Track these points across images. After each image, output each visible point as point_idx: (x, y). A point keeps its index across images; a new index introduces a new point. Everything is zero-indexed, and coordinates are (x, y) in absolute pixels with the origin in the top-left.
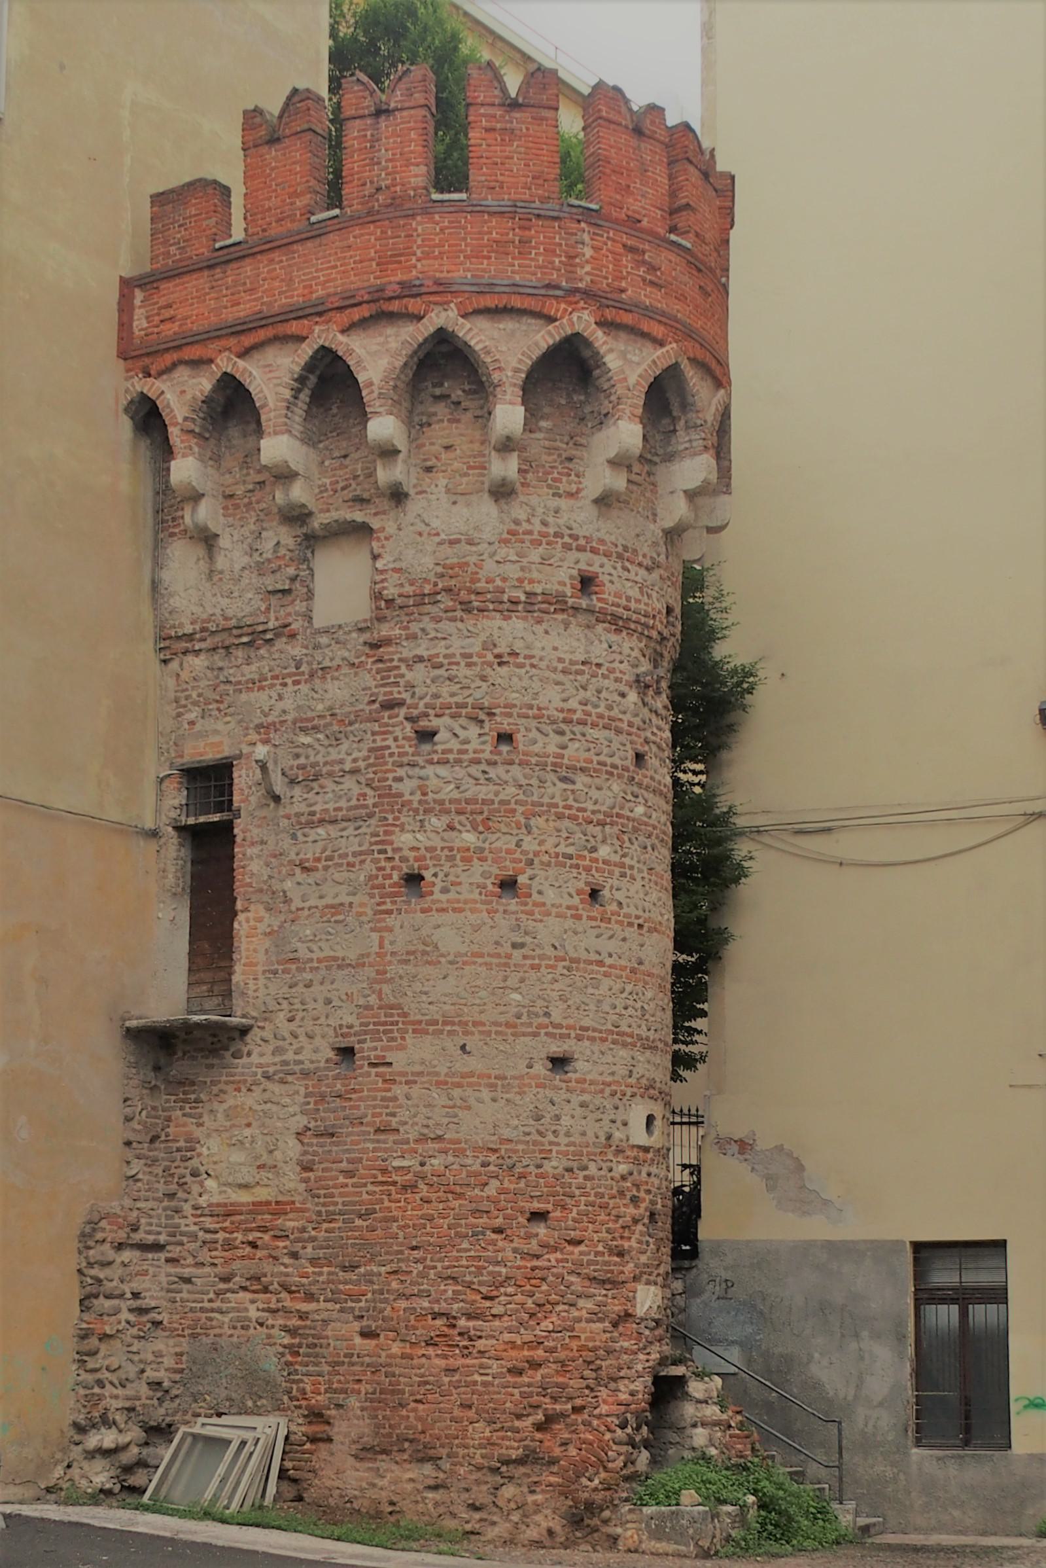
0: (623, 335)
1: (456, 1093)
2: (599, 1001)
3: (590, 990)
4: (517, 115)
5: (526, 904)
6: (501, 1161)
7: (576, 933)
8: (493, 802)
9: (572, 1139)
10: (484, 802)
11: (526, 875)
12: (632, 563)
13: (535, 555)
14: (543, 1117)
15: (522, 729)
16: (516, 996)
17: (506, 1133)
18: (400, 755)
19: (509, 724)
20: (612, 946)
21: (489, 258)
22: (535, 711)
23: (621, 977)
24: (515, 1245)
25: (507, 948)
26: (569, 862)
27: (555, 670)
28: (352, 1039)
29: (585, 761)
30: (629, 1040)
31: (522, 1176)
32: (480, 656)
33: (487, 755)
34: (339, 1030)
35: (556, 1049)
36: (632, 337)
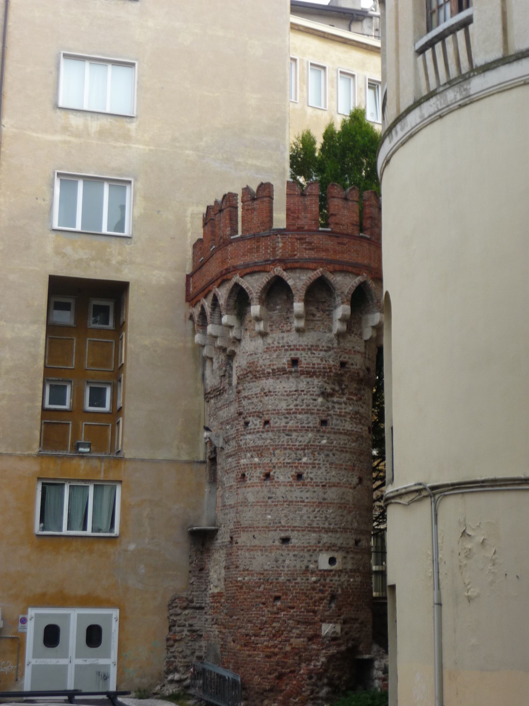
0: (298, 271)
1: (252, 553)
4: (256, 202)
5: (272, 482)
7: (291, 491)
8: (262, 446)
9: (290, 569)
10: (260, 446)
12: (316, 350)
13: (275, 356)
15: (273, 418)
16: (269, 517)
17: (266, 567)
21: (247, 255)
22: (277, 411)
24: (269, 609)
25: (267, 499)
26: (288, 466)
27: (284, 395)
29: (296, 427)
30: (317, 529)
31: (271, 583)
32: (260, 394)
33: (261, 430)
35: (283, 535)
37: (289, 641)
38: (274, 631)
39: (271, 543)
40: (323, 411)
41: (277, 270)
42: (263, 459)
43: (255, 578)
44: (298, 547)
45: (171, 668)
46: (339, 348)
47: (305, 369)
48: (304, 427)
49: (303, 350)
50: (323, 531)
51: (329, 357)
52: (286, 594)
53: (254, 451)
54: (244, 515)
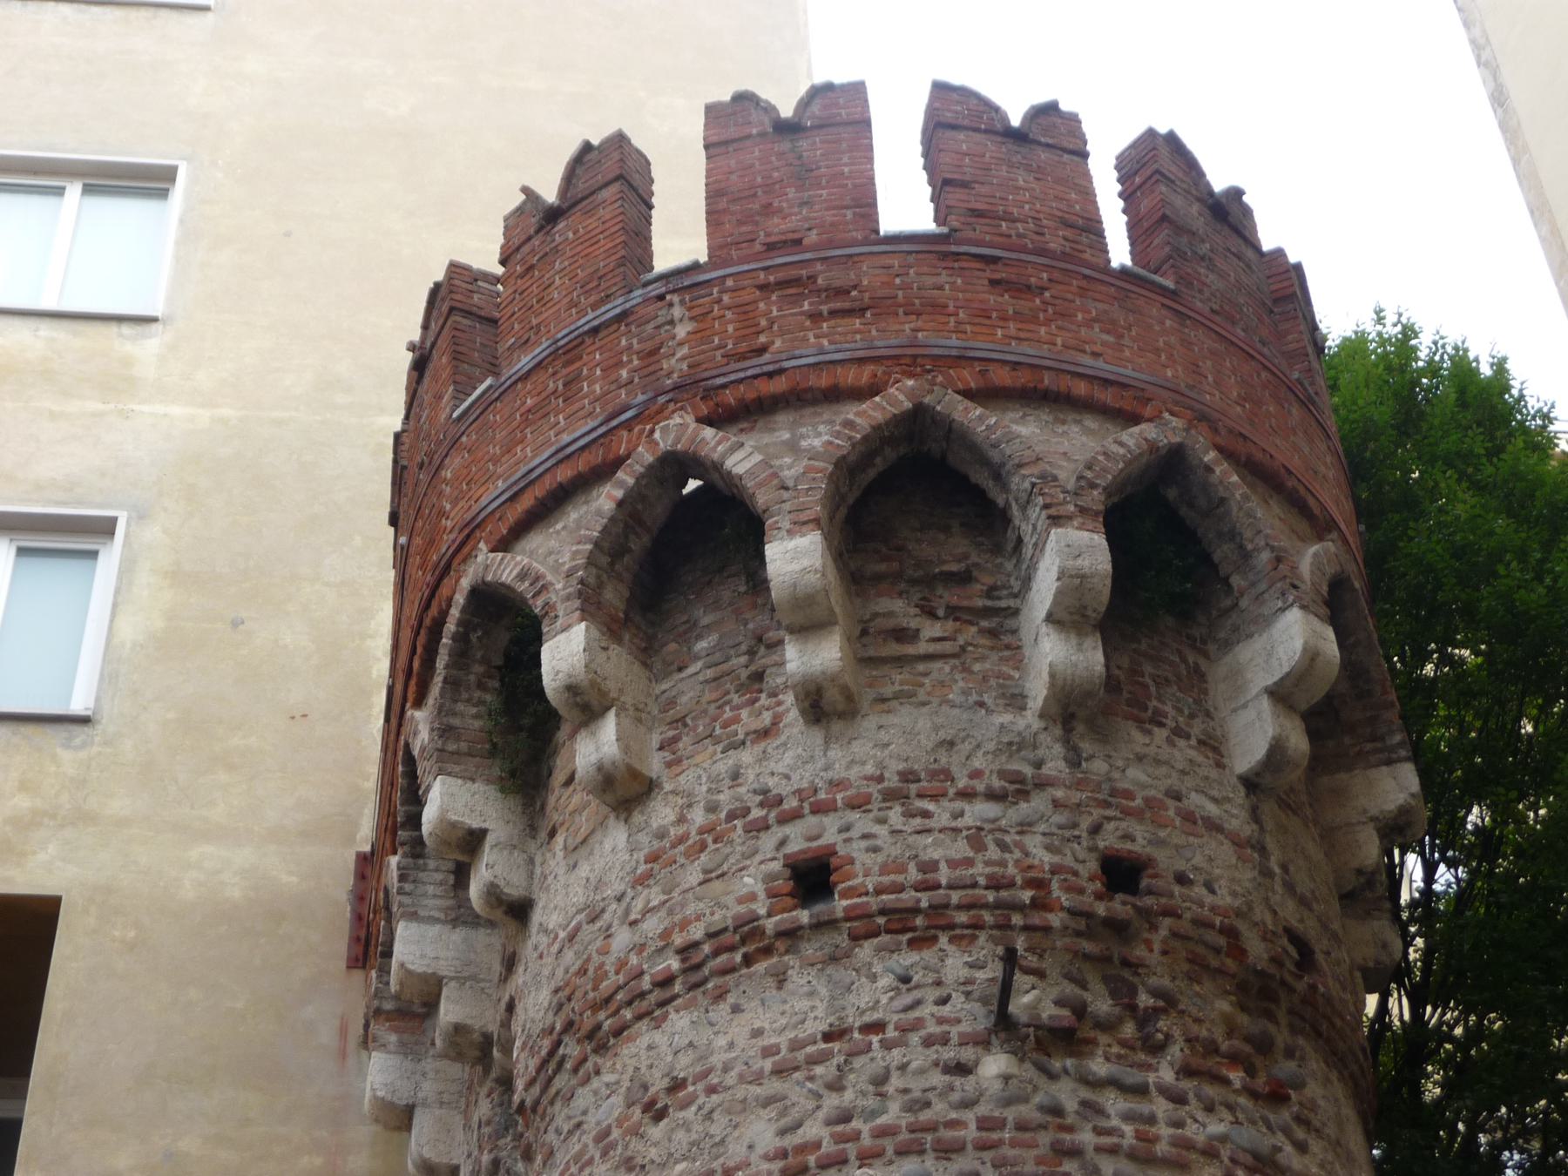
0: (782, 418)
12: (934, 797)
13: (693, 876)
36: (808, 411)
40: (1021, 1127)
41: (665, 430)
46: (1079, 785)
47: (874, 903)
51: (1025, 827)
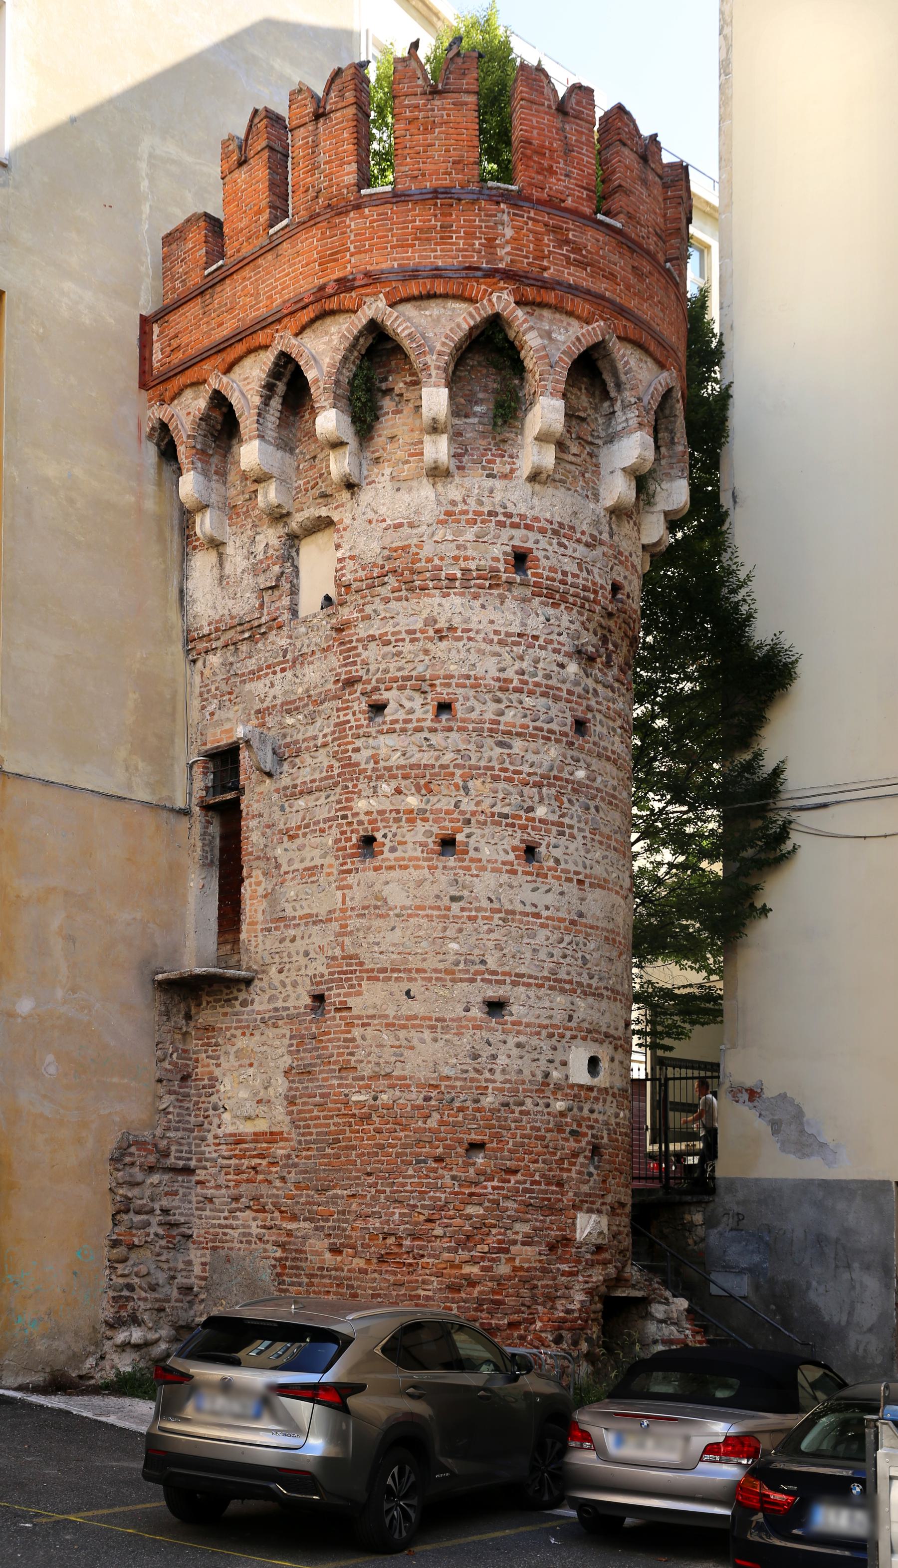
1: (402, 1034)
2: (534, 950)
3: (526, 941)
5: (463, 860)
6: (440, 1096)
7: (511, 887)
8: (433, 766)
9: (508, 1077)
11: (463, 834)
12: (570, 539)
14: (479, 1056)
15: (461, 699)
16: (454, 946)
17: (446, 1071)
18: (358, 727)
19: (448, 694)
20: (550, 899)
22: (472, 681)
23: (559, 928)
25: (446, 901)
26: (504, 821)
28: (324, 987)
29: (523, 726)
30: (567, 986)
32: (422, 632)
33: (428, 724)
34: (315, 980)
35: (492, 992)
37: (507, 1251)
38: (467, 1228)
39: (459, 1011)
42: (435, 799)
43: (413, 1096)
44: (528, 1025)
45: (123, 1313)
48: (541, 730)
49: (542, 531)
50: (579, 991)
52: (498, 1137)
53: (405, 777)
54: (371, 938)
